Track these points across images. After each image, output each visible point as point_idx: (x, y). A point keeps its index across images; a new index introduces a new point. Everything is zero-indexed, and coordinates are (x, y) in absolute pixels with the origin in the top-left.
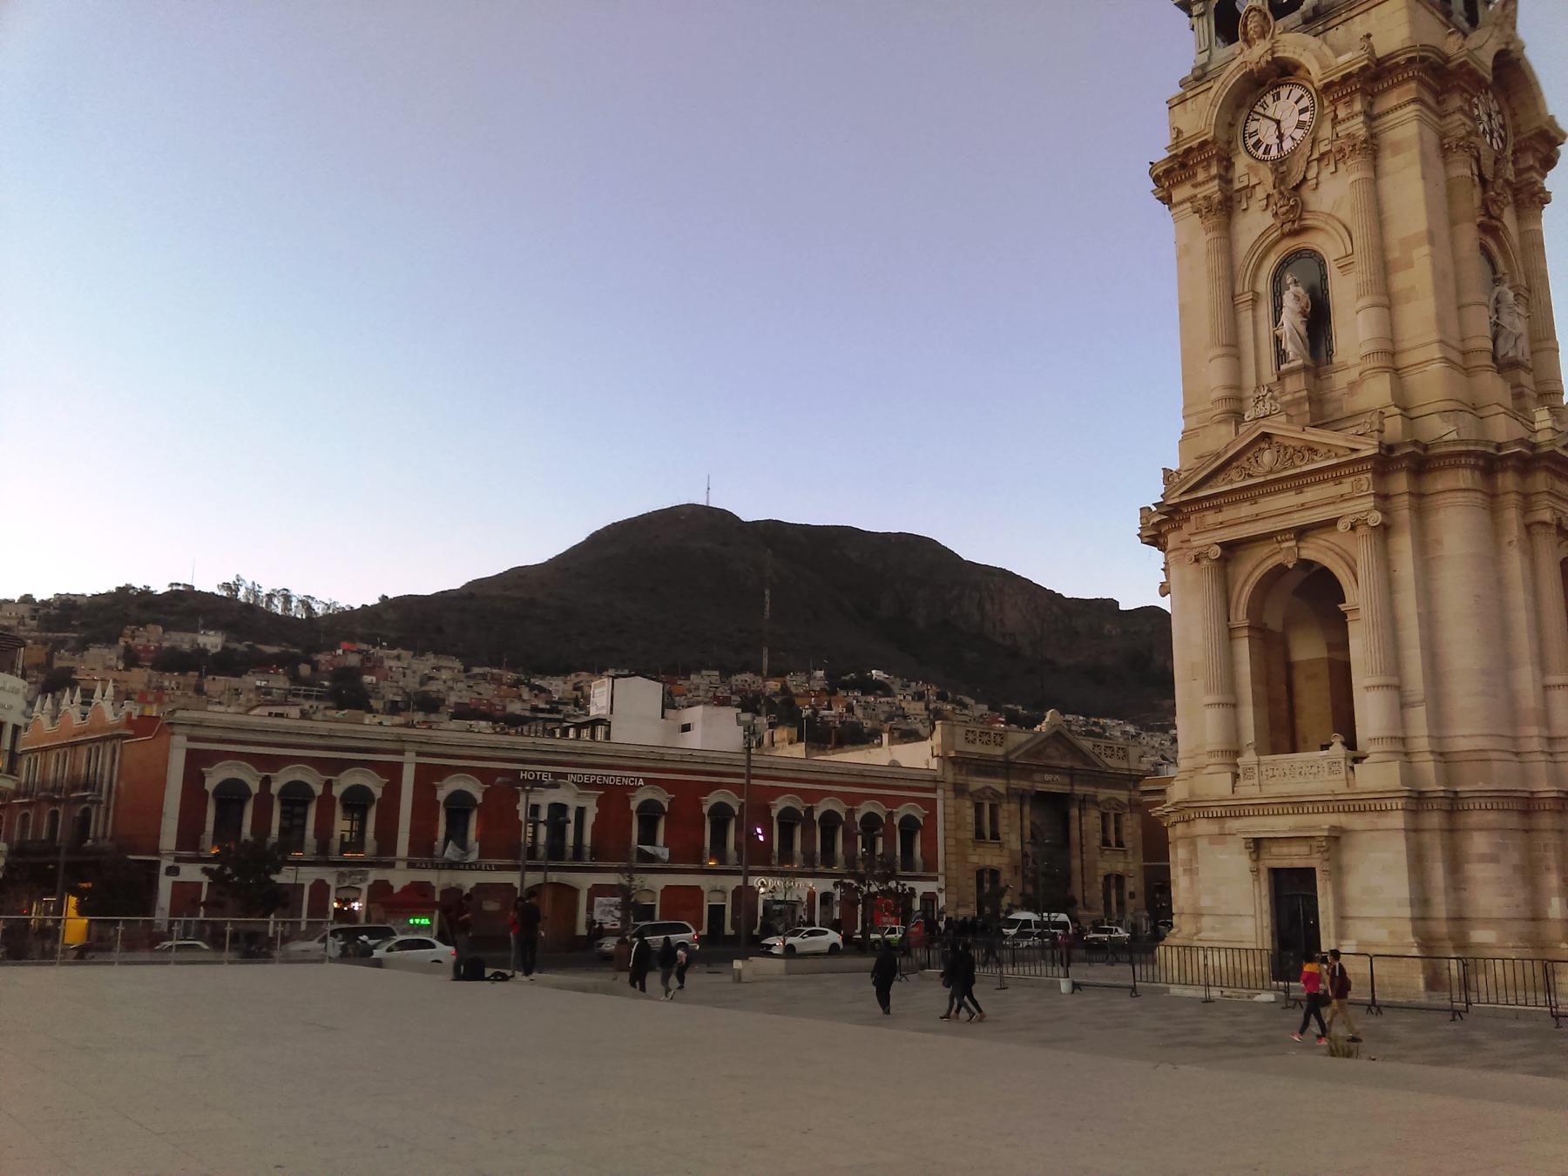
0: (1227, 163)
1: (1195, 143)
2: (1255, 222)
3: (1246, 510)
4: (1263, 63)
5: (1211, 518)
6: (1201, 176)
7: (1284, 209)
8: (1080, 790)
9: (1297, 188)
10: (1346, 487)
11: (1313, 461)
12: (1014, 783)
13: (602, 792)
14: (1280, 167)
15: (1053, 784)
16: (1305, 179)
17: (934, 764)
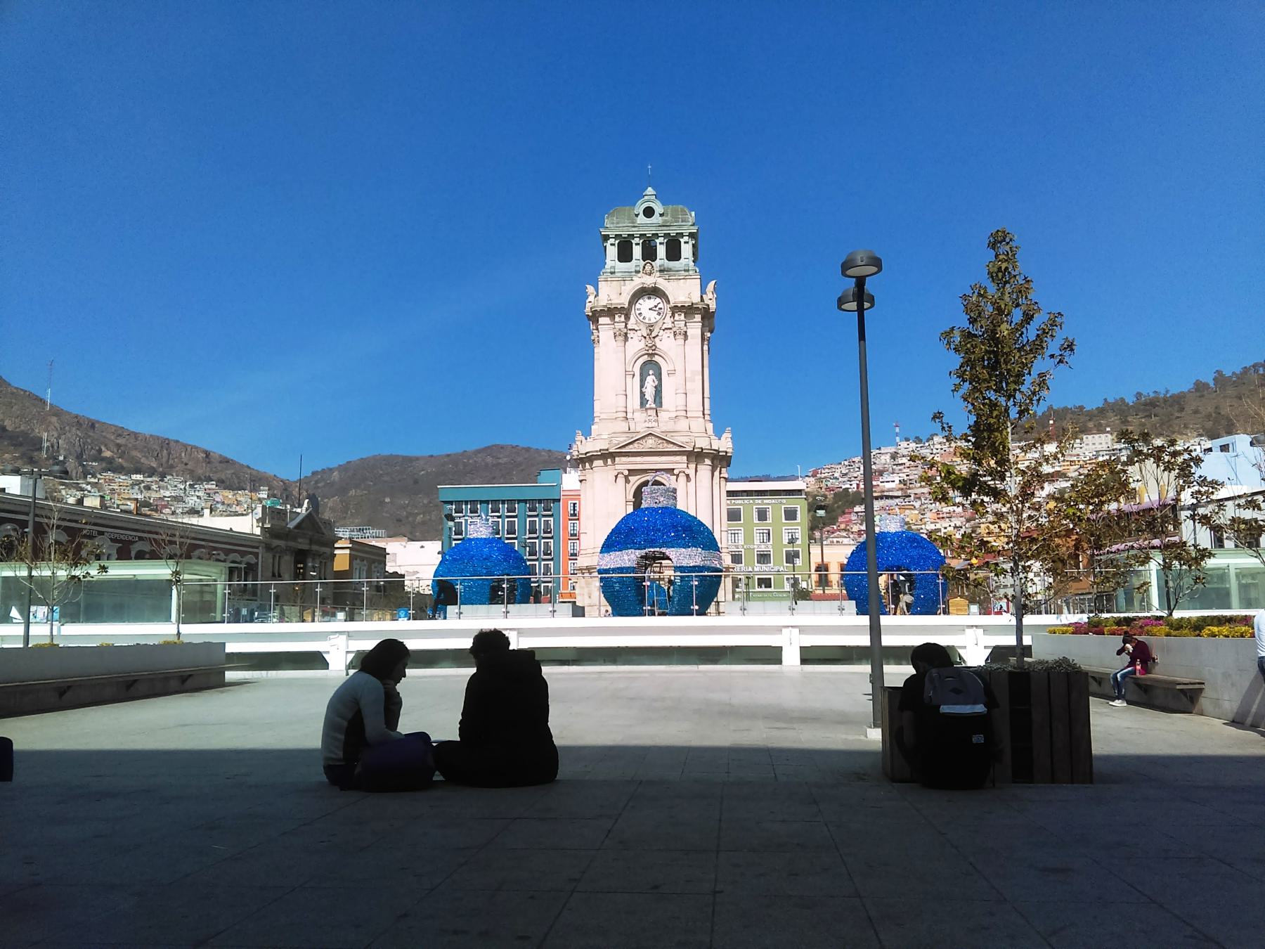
0: (627, 317)
1: (619, 307)
2: (636, 344)
3: (638, 459)
4: (650, 286)
5: (624, 459)
6: (617, 319)
7: (650, 345)
8: (315, 548)
9: (654, 338)
10: (678, 458)
11: (667, 448)
12: (291, 544)
13: (121, 545)
14: (651, 327)
15: (303, 544)
16: (658, 335)
17: (258, 531)
